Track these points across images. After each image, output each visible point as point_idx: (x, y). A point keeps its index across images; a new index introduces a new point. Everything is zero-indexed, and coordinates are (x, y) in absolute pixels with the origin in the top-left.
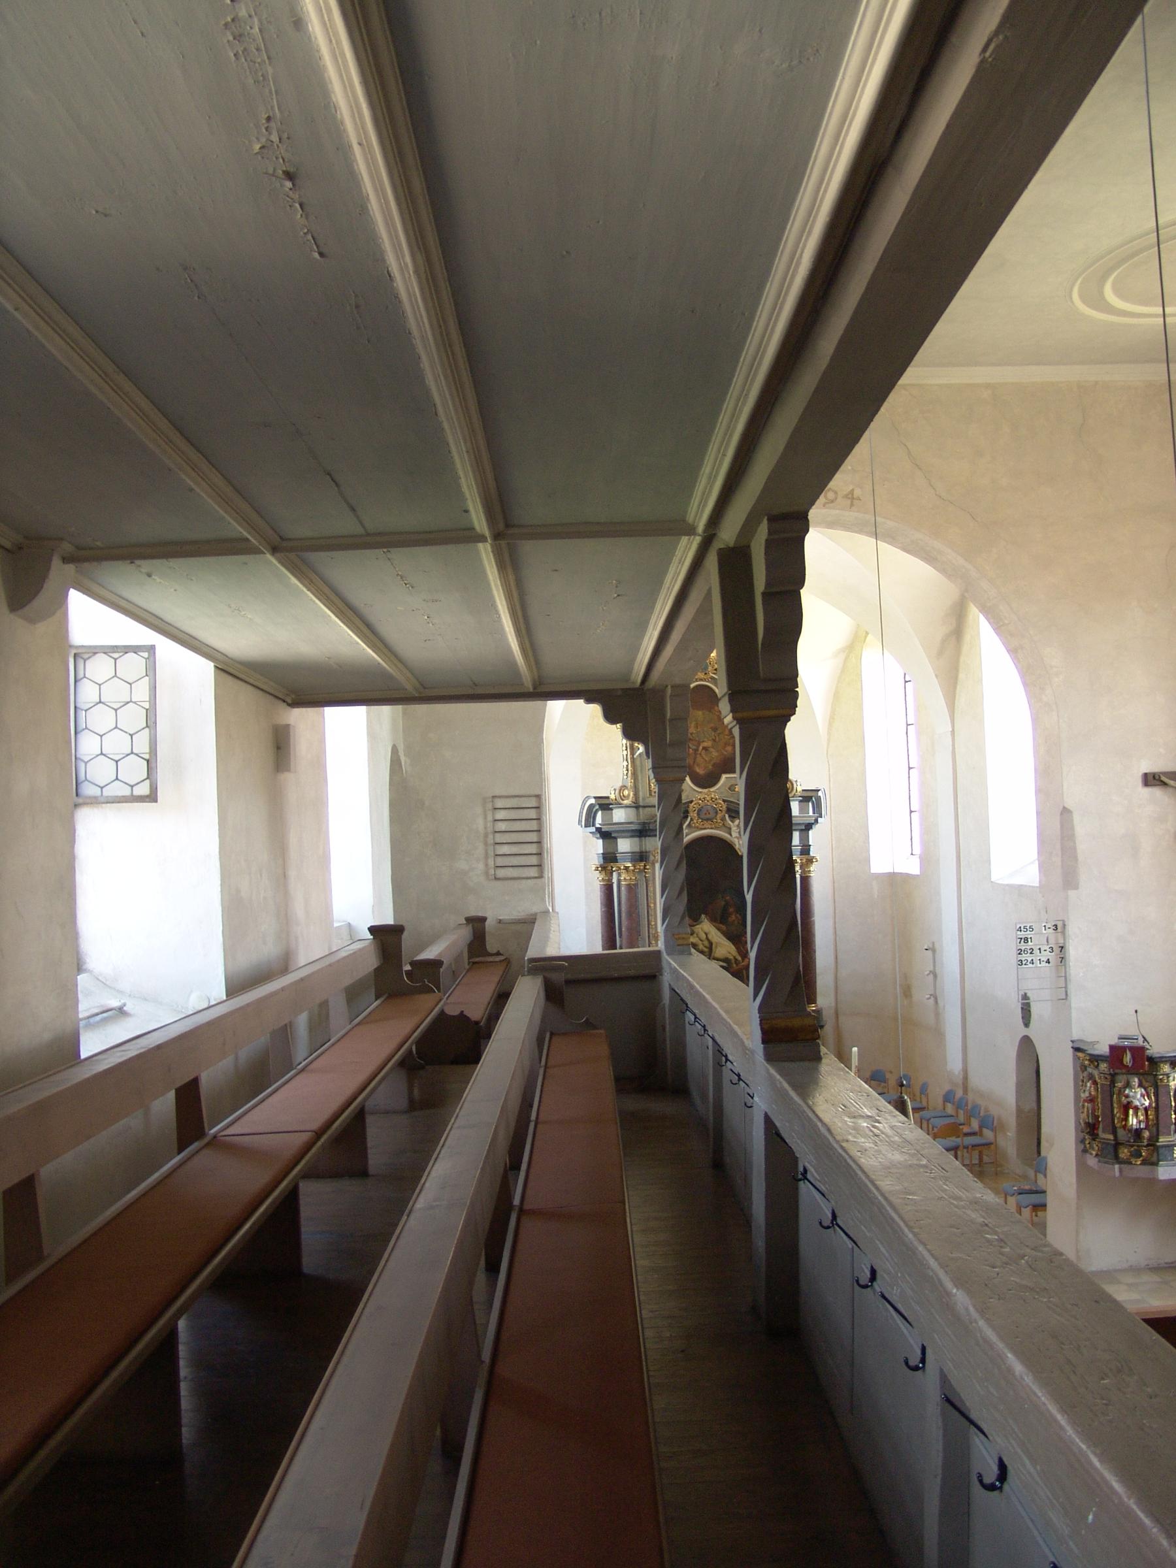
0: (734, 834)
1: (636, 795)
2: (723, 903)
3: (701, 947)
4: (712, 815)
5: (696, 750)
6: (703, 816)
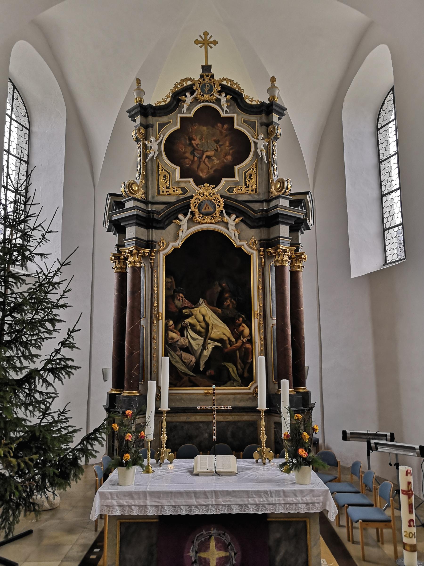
0: (230, 227)
1: (146, 193)
2: (220, 289)
3: (198, 328)
4: (212, 210)
5: (201, 158)
6: (203, 211)
